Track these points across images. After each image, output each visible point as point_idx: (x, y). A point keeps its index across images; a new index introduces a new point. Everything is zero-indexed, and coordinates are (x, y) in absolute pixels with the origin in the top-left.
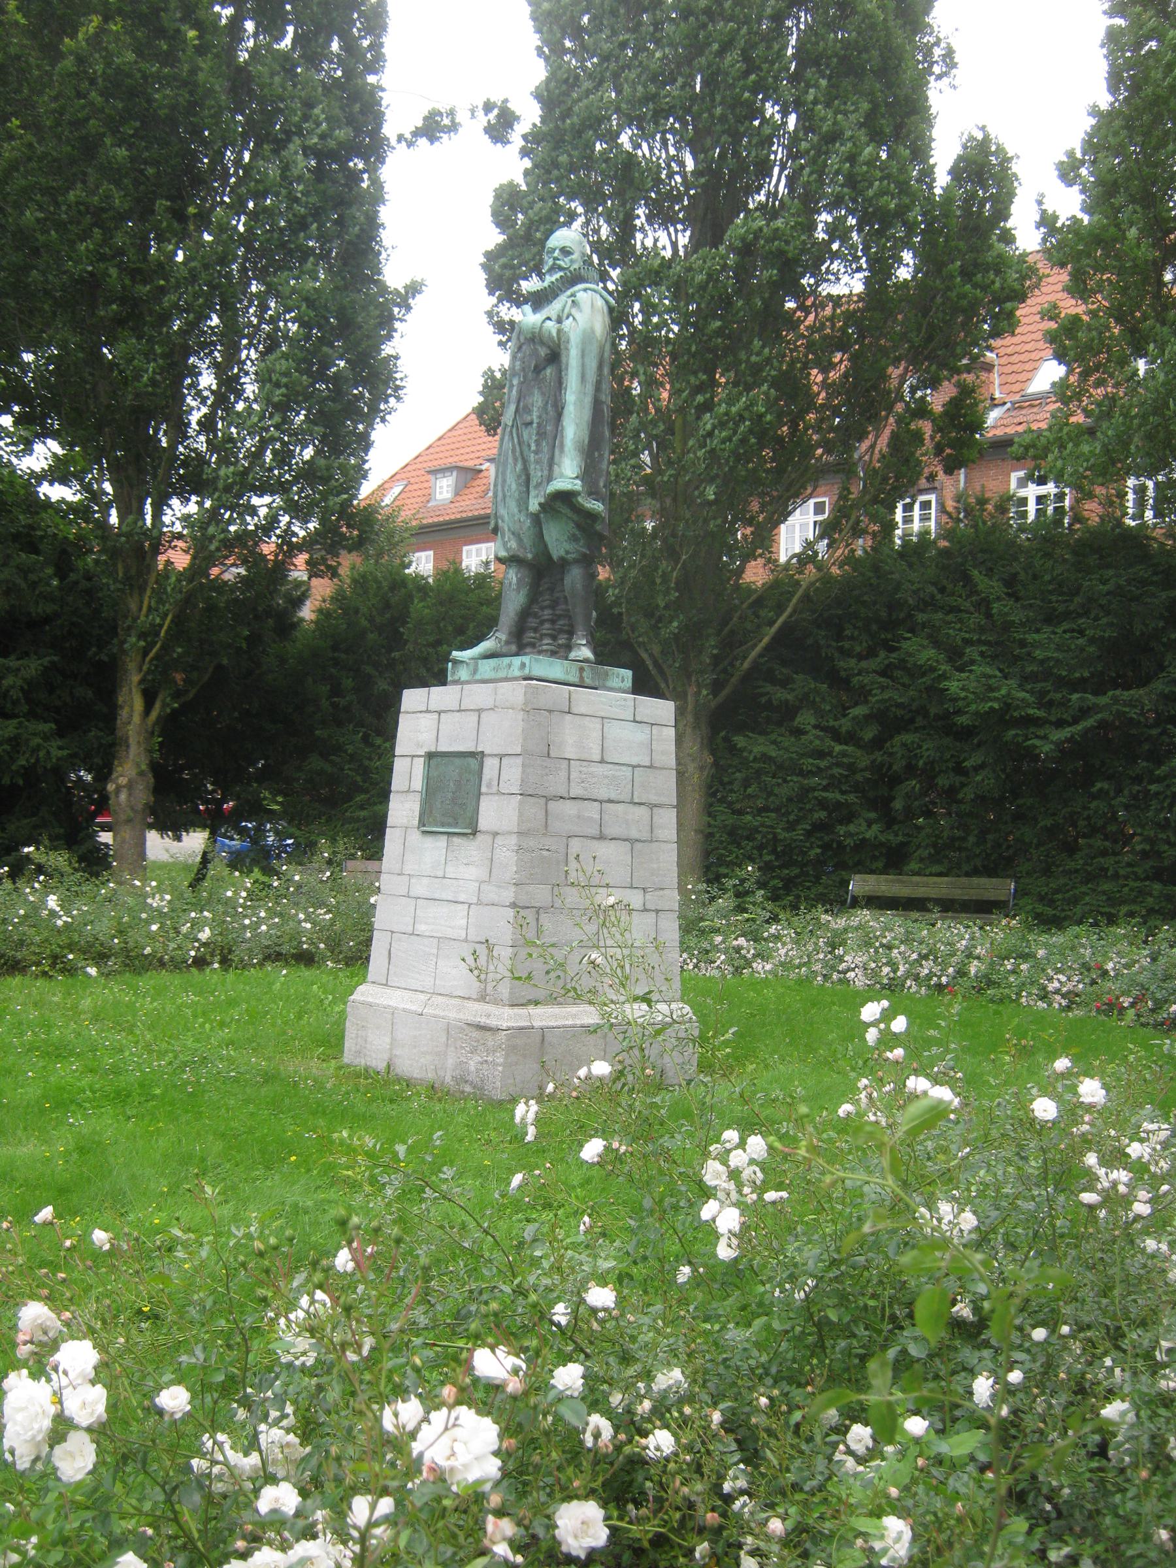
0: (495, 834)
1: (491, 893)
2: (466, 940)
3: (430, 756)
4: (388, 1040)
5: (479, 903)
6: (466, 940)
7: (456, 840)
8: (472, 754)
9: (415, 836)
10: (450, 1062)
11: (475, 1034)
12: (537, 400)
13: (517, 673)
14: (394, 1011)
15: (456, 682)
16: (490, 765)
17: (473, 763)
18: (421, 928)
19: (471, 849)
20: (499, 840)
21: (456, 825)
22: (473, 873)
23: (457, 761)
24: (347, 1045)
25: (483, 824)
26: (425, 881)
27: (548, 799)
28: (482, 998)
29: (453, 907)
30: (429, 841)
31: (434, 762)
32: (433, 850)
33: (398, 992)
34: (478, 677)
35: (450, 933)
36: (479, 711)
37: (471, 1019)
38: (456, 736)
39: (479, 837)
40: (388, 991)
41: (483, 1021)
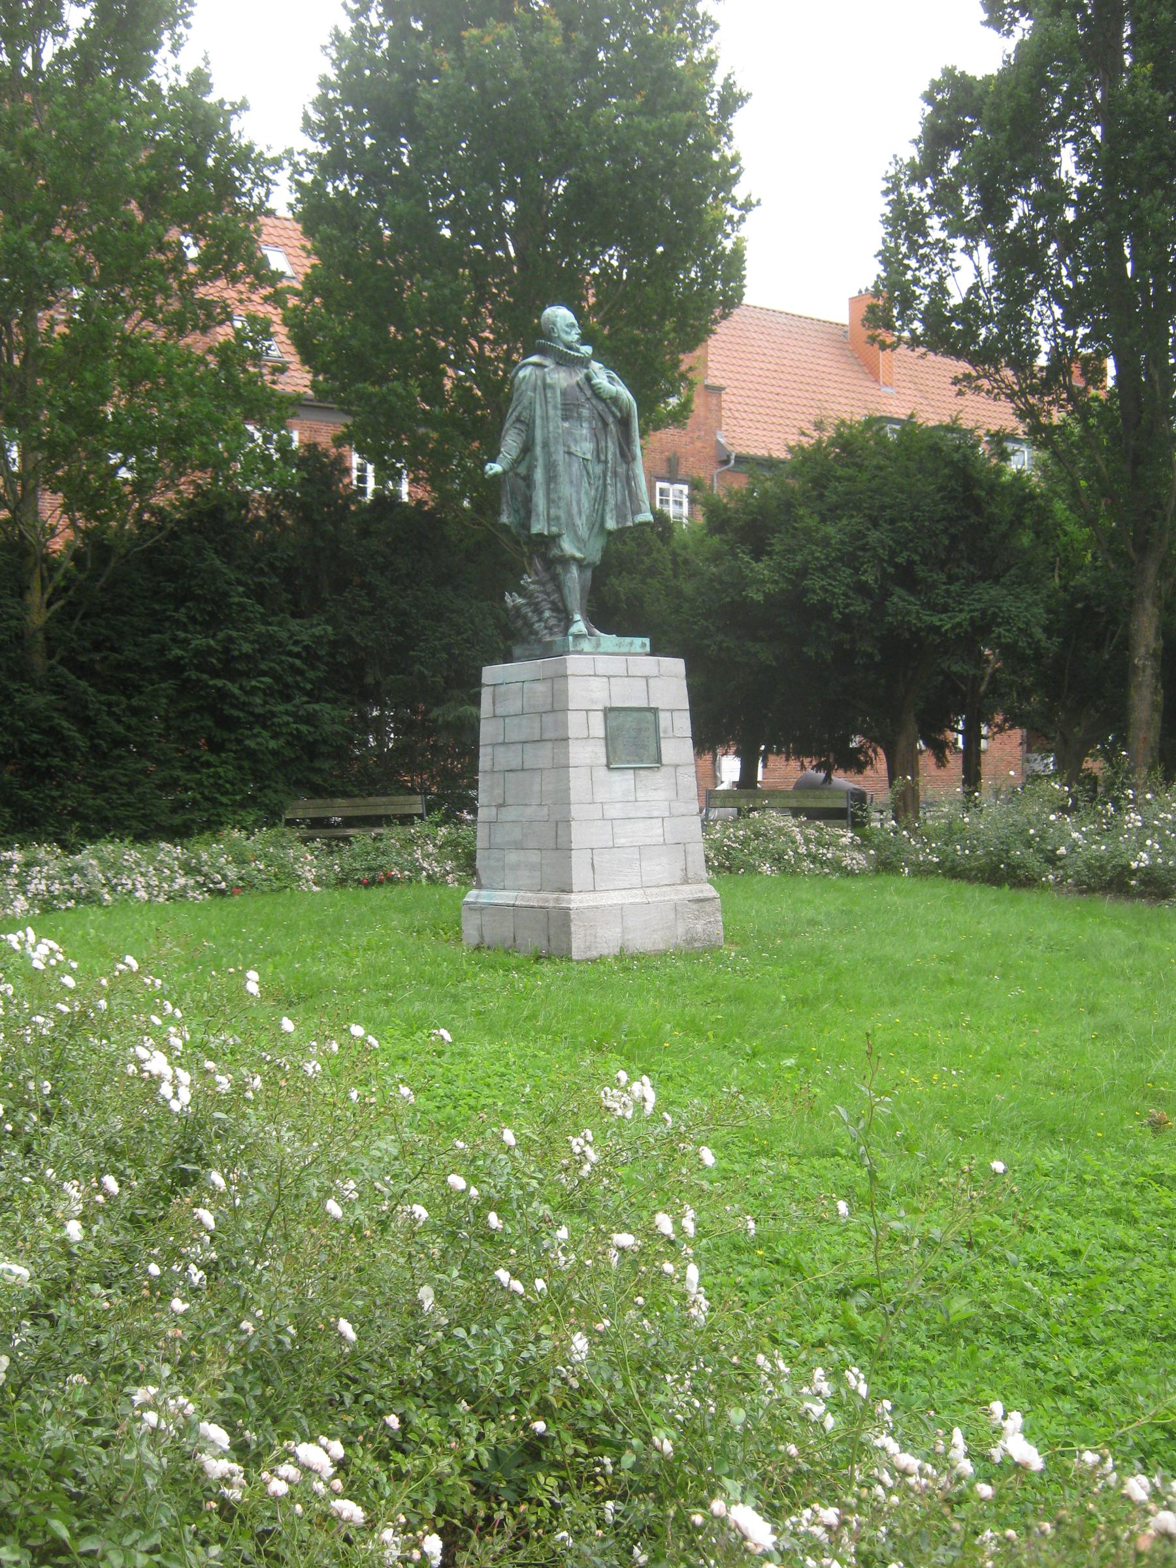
0: (677, 766)
1: (680, 808)
2: (665, 844)
3: (608, 711)
4: (619, 930)
5: (671, 816)
6: (665, 844)
7: (642, 772)
8: (649, 709)
9: (602, 773)
10: (681, 930)
11: (695, 906)
12: (612, 448)
13: (639, 650)
14: (622, 907)
15: (581, 652)
16: (664, 719)
17: (650, 716)
18: (621, 841)
19: (659, 778)
20: (680, 770)
21: (642, 761)
22: (661, 795)
23: (635, 714)
24: (574, 945)
25: (665, 759)
26: (619, 805)
27: (504, 743)
28: (686, 881)
29: (648, 822)
30: (616, 776)
31: (611, 715)
32: (621, 782)
33: (606, 894)
34: (601, 650)
35: (648, 841)
36: (647, 678)
37: (691, 897)
38: (630, 695)
39: (663, 769)
40: (597, 895)
41: (701, 895)
